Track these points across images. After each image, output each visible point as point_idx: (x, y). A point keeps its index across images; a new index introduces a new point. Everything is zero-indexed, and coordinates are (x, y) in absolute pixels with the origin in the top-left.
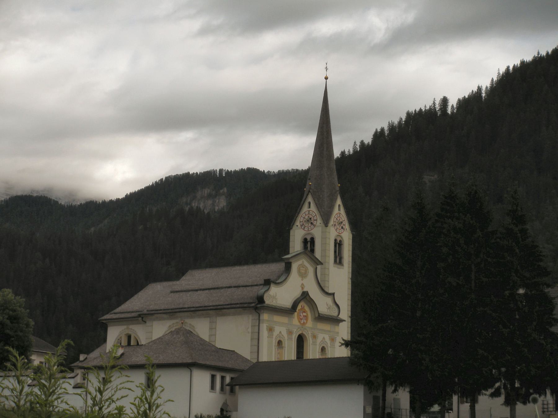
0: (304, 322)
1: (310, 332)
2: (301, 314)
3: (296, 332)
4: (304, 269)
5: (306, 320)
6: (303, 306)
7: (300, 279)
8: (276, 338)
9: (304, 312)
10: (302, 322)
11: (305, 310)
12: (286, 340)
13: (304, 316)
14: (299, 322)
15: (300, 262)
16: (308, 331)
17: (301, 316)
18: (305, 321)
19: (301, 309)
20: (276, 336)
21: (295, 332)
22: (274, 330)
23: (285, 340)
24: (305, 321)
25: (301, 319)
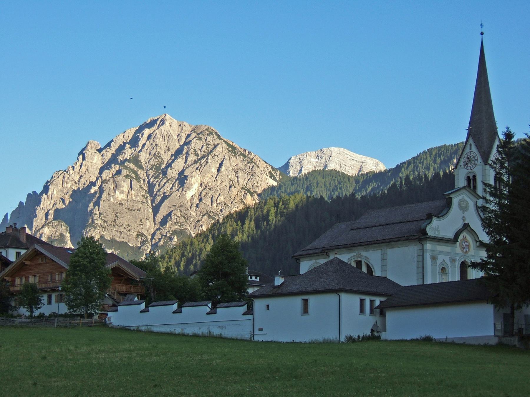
0: (466, 251)
2: (464, 244)
3: (459, 259)
4: (464, 203)
5: (468, 248)
6: (465, 236)
7: (461, 212)
9: (466, 242)
10: (465, 251)
11: (467, 239)
12: (450, 267)
13: (466, 245)
14: (462, 250)
15: (460, 197)
17: (463, 245)
18: (467, 250)
19: (463, 239)
20: (440, 264)
22: (437, 259)
23: (449, 267)
24: (467, 250)
25: (463, 248)
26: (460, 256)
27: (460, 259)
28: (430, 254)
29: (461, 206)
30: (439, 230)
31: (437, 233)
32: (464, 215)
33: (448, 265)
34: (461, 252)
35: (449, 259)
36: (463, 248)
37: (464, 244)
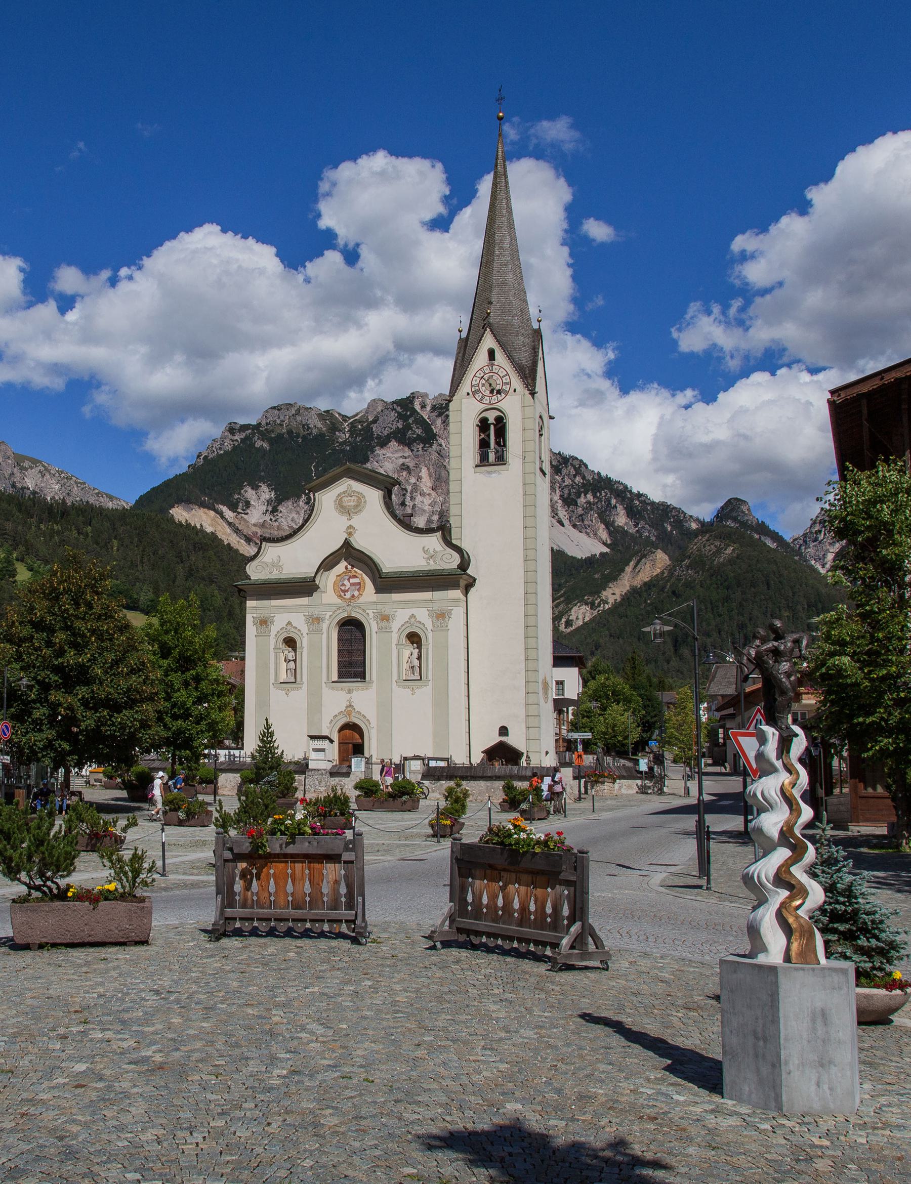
0: (353, 596)
1: (370, 612)
2: (346, 582)
4: (353, 498)
5: (358, 590)
7: (344, 518)
8: (278, 635)
10: (348, 595)
12: (305, 635)
13: (352, 584)
16: (364, 610)
17: (343, 585)
18: (356, 593)
20: (278, 632)
21: (327, 617)
22: (272, 623)
23: (302, 634)
24: (356, 593)
25: (345, 591)
26: (335, 608)
27: (334, 616)
28: (255, 615)
29: (342, 507)
30: (281, 564)
31: (275, 572)
32: (352, 523)
33: (299, 630)
34: (339, 601)
35: (304, 618)
36: (345, 591)
37: (346, 582)
